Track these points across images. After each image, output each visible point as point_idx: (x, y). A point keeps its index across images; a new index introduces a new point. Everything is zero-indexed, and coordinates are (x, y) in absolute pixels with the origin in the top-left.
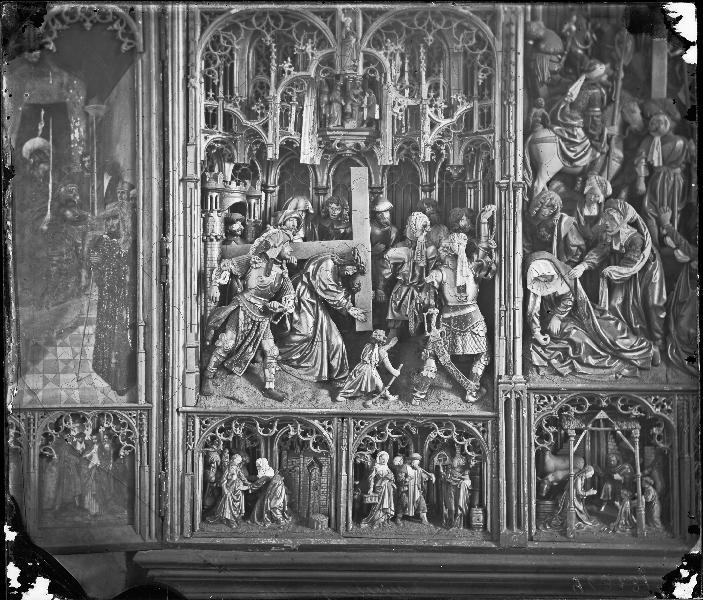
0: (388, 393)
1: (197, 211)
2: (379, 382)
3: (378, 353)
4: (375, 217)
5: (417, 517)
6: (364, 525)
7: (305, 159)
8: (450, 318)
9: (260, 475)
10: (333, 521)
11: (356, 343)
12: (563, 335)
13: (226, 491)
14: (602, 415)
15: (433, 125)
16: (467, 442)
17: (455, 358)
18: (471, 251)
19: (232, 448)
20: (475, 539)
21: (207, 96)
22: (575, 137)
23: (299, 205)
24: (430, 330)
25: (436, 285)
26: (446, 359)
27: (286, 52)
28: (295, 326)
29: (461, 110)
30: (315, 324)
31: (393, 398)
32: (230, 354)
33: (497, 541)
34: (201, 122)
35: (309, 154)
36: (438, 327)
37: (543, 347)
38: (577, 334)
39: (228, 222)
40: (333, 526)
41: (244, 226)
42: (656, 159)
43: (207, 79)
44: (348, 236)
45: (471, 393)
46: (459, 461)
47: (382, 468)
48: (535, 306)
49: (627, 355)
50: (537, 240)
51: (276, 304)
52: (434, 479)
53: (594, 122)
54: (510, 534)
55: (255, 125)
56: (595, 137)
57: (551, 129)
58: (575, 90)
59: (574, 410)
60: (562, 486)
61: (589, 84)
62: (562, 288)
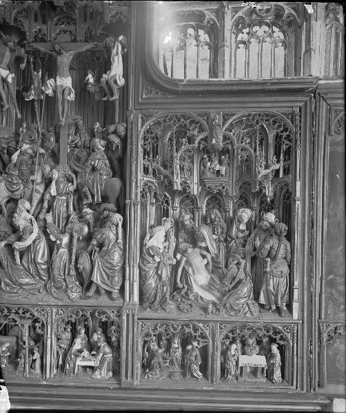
49: (24, 287)
53: (22, 172)
56: (25, 182)
58: (15, 157)
61: (22, 153)
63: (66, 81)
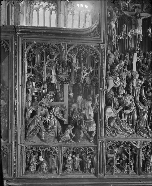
0: (72, 140)
1: (25, 94)
2: (70, 138)
3: (69, 131)
4: (69, 96)
5: (78, 170)
6: (65, 172)
7: (52, 82)
8: (87, 123)
9: (40, 160)
10: (58, 172)
11: (64, 128)
12: (114, 126)
13: (31, 164)
14: (122, 146)
15: (84, 74)
16: (90, 152)
17: (88, 132)
18: (93, 106)
19: (34, 153)
20: (92, 176)
21: (28, 65)
22: (116, 78)
23: (52, 93)
24: (82, 125)
25: (84, 114)
26: (86, 132)
27: (48, 53)
28: (49, 123)
29: (91, 71)
30: (54, 122)
31: (73, 141)
32: (33, 130)
33: (97, 176)
34: (26, 71)
35: (54, 80)
36: (84, 124)
37: (109, 130)
38: (116, 126)
39: (33, 97)
40: (57, 173)
41: (37, 99)
42: (135, 85)
43: (28, 61)
44: (63, 101)
45: (92, 141)
46: (88, 157)
47: (70, 158)
48: (107, 119)
50: (108, 104)
51: (44, 118)
52: (82, 160)
54: (101, 175)
55: (40, 72)
56: (121, 79)
57: (112, 76)
58: (117, 67)
59: (115, 145)
60: (112, 161)
62: (114, 115)
63: (139, 31)
